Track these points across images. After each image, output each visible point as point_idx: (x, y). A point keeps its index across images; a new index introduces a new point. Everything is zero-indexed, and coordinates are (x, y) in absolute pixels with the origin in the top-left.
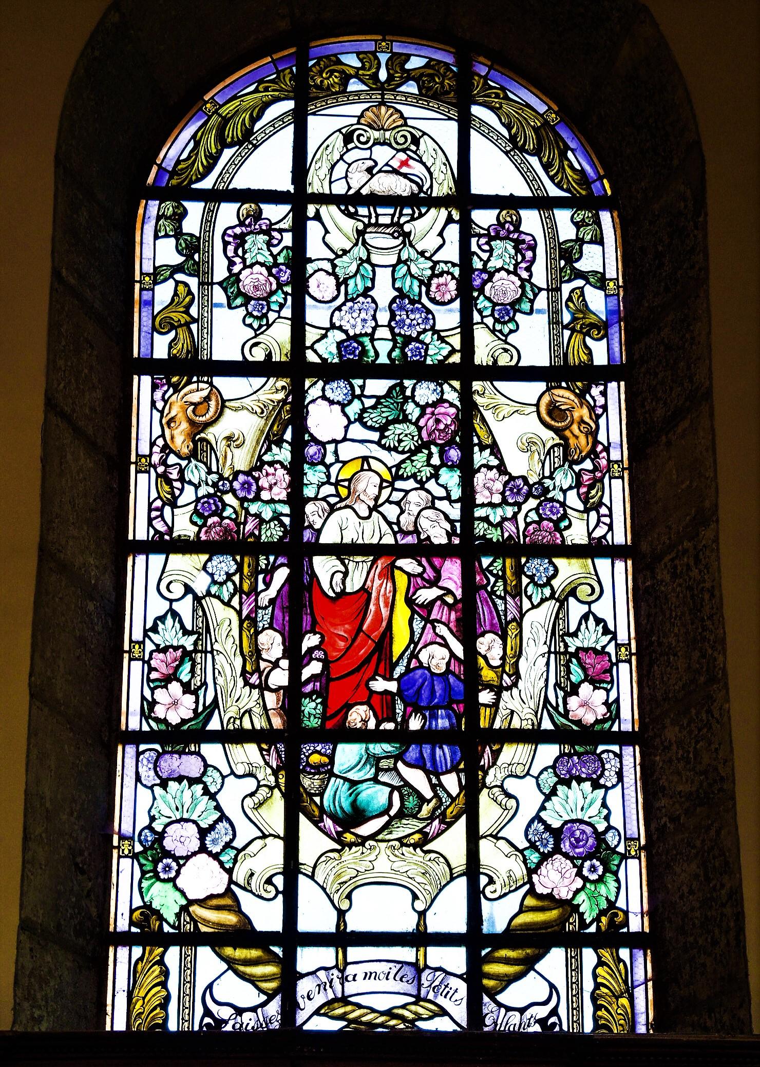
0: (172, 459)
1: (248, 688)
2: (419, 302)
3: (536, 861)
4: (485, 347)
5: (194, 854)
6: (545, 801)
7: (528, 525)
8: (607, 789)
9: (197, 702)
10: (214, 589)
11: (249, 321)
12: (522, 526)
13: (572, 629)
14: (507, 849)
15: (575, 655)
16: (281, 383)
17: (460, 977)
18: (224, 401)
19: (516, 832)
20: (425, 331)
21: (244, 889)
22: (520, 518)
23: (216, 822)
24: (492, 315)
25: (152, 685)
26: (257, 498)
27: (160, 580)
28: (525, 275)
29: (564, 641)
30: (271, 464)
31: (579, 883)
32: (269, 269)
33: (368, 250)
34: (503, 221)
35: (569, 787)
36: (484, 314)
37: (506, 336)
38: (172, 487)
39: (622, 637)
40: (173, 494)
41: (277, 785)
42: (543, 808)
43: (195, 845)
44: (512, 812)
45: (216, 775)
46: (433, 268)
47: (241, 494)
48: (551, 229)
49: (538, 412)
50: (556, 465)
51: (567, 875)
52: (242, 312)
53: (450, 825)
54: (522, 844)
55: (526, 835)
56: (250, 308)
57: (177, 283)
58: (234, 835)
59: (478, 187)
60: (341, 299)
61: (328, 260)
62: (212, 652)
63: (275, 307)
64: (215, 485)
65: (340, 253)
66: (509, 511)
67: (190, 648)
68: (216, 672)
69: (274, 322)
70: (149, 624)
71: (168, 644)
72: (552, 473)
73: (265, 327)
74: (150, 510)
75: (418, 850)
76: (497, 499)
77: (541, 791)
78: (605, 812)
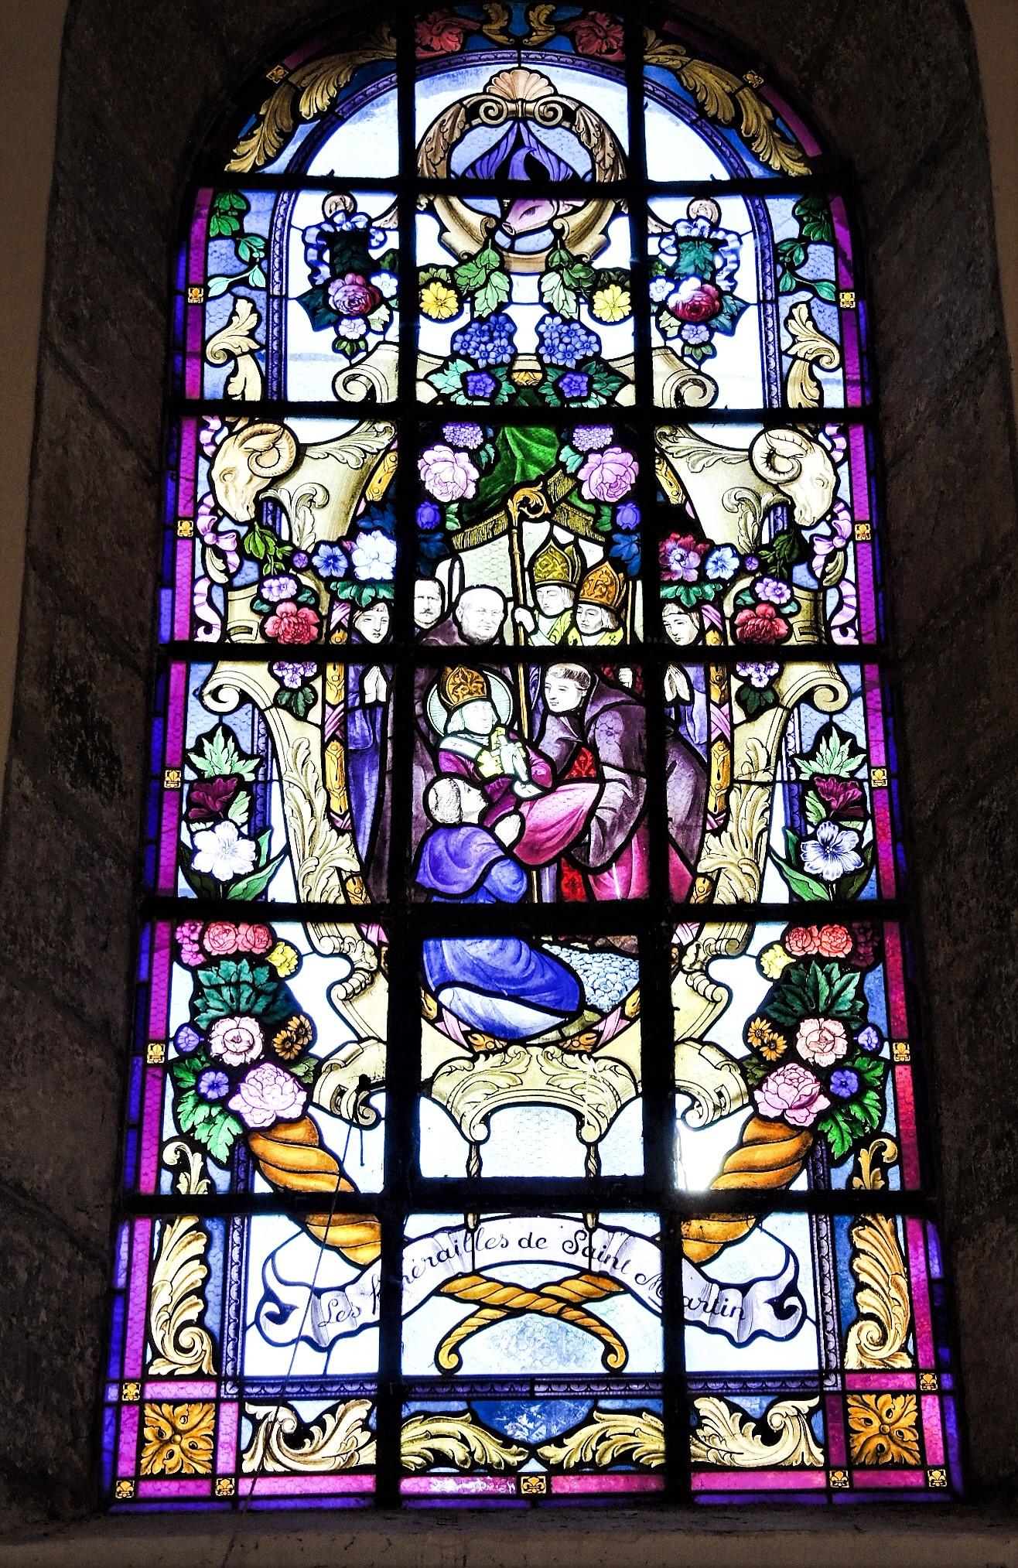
5: (256, 1064)
7: (738, 609)
9: (258, 851)
12: (728, 610)
14: (717, 1057)
17: (652, 1240)
21: (331, 1114)
24: (679, 335)
28: (724, 285)
29: (795, 765)
34: (693, 216)
37: (700, 363)
45: (290, 953)
47: (324, 573)
48: (761, 223)
49: (750, 458)
54: (740, 1051)
55: (746, 1037)
56: (343, 330)
62: (280, 780)
67: (250, 778)
69: (376, 348)
70: (190, 743)
72: (772, 541)
73: (362, 355)
77: (765, 976)
78: (860, 1004)
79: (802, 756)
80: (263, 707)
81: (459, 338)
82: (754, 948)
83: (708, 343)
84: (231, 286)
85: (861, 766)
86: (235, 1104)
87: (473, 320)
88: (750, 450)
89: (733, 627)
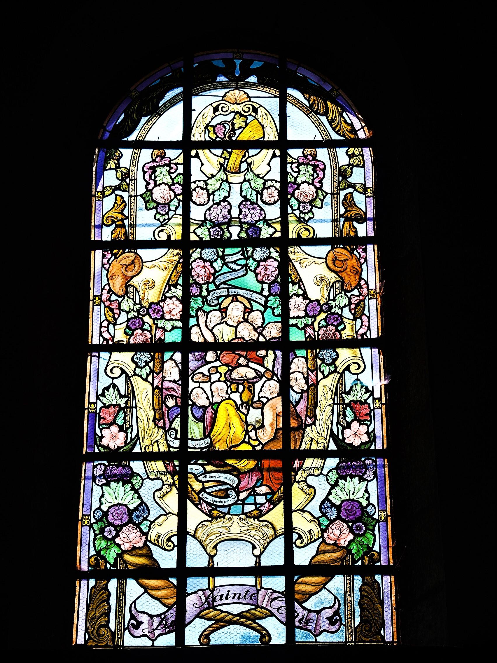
0: (114, 298)
1: (156, 428)
2: (256, 204)
3: (326, 524)
4: (294, 229)
5: (126, 524)
6: (331, 489)
8: (368, 481)
10: (138, 371)
11: (158, 216)
12: (317, 329)
13: (347, 389)
14: (310, 517)
15: (349, 405)
16: (176, 252)
18: (143, 262)
19: (314, 507)
20: (260, 220)
22: (316, 324)
23: (139, 506)
24: (298, 209)
25: (101, 427)
26: (163, 318)
27: (107, 366)
28: (318, 185)
29: (342, 397)
30: (171, 298)
31: (351, 537)
32: (170, 187)
33: (226, 174)
35: (346, 481)
36: (294, 208)
38: (114, 313)
39: (377, 395)
40: (114, 317)
41: (174, 484)
42: (330, 493)
43: (126, 519)
44: (311, 497)
45: (139, 478)
46: (264, 184)
48: (334, 158)
50: (337, 293)
51: (344, 532)
52: (154, 211)
53: (275, 506)
54: (318, 514)
57: (116, 196)
58: (149, 513)
59: (291, 136)
60: (211, 203)
61: (204, 181)
62: (136, 407)
63: (173, 208)
64: (138, 311)
65: (210, 176)
66: (310, 321)
68: (138, 419)
69: (172, 217)
70: (100, 392)
71: (110, 403)
74: (101, 327)
75: (256, 520)
76: (302, 314)
77: (329, 483)
78: (367, 495)
79: (346, 393)
80: (130, 375)
81: (208, 212)
82: (325, 472)
83: (310, 211)
84: (113, 192)
85: (369, 397)
86: (118, 541)
87: (214, 204)
88: (326, 258)
89: (318, 335)
